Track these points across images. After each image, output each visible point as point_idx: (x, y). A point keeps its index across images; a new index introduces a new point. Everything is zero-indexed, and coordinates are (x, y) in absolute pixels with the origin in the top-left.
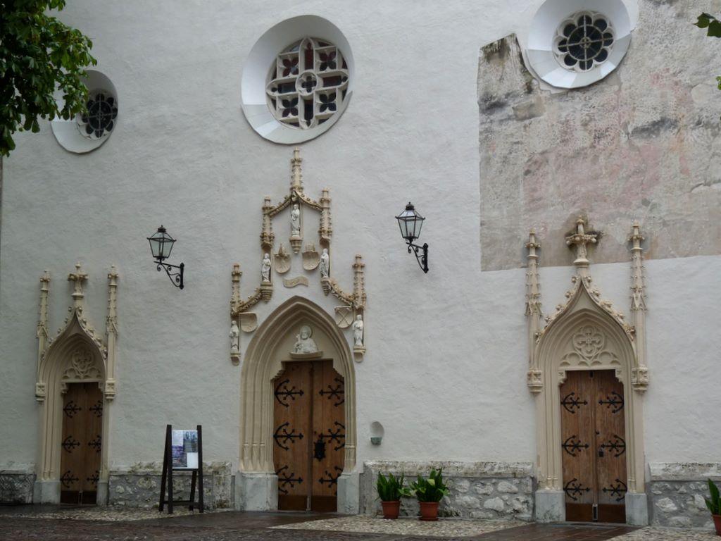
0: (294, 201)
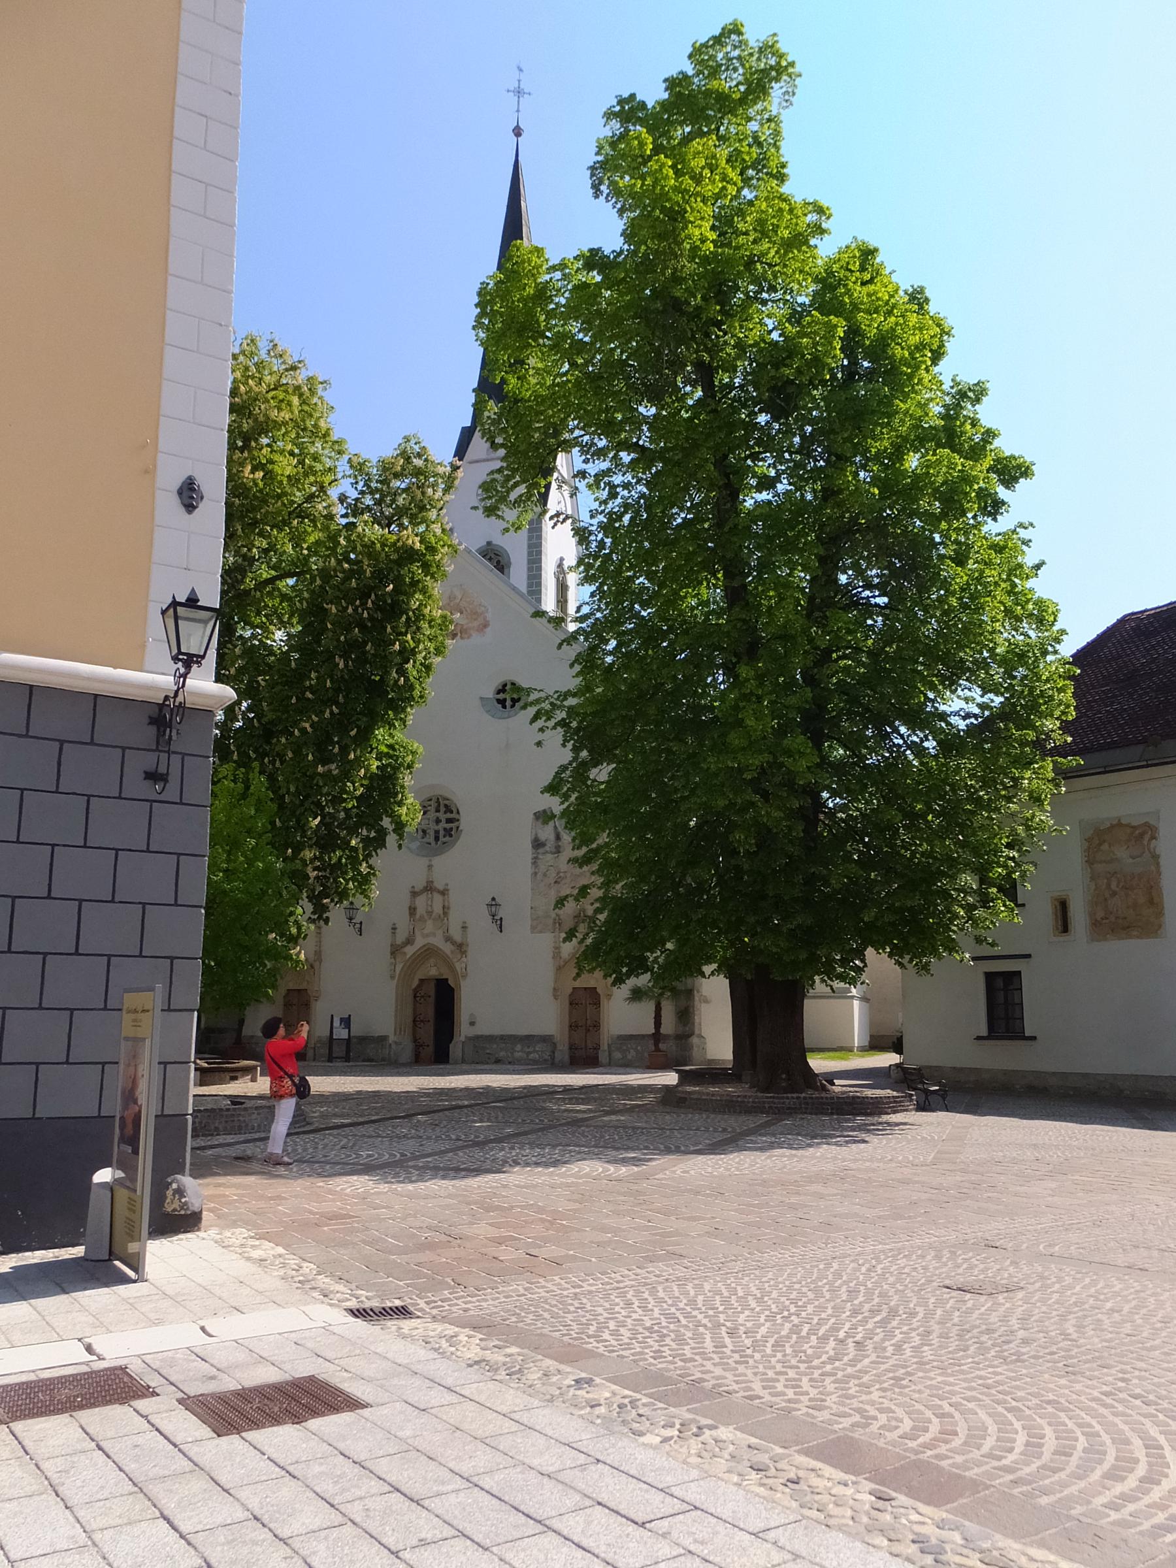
0: (429, 888)
